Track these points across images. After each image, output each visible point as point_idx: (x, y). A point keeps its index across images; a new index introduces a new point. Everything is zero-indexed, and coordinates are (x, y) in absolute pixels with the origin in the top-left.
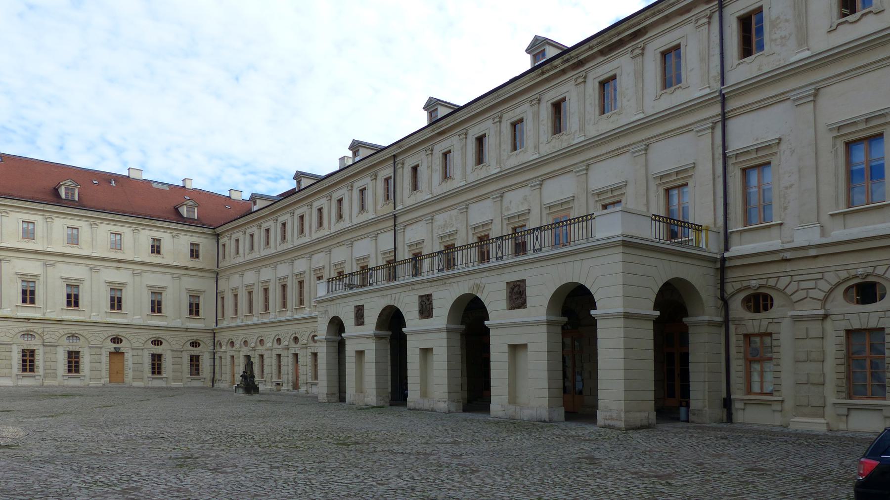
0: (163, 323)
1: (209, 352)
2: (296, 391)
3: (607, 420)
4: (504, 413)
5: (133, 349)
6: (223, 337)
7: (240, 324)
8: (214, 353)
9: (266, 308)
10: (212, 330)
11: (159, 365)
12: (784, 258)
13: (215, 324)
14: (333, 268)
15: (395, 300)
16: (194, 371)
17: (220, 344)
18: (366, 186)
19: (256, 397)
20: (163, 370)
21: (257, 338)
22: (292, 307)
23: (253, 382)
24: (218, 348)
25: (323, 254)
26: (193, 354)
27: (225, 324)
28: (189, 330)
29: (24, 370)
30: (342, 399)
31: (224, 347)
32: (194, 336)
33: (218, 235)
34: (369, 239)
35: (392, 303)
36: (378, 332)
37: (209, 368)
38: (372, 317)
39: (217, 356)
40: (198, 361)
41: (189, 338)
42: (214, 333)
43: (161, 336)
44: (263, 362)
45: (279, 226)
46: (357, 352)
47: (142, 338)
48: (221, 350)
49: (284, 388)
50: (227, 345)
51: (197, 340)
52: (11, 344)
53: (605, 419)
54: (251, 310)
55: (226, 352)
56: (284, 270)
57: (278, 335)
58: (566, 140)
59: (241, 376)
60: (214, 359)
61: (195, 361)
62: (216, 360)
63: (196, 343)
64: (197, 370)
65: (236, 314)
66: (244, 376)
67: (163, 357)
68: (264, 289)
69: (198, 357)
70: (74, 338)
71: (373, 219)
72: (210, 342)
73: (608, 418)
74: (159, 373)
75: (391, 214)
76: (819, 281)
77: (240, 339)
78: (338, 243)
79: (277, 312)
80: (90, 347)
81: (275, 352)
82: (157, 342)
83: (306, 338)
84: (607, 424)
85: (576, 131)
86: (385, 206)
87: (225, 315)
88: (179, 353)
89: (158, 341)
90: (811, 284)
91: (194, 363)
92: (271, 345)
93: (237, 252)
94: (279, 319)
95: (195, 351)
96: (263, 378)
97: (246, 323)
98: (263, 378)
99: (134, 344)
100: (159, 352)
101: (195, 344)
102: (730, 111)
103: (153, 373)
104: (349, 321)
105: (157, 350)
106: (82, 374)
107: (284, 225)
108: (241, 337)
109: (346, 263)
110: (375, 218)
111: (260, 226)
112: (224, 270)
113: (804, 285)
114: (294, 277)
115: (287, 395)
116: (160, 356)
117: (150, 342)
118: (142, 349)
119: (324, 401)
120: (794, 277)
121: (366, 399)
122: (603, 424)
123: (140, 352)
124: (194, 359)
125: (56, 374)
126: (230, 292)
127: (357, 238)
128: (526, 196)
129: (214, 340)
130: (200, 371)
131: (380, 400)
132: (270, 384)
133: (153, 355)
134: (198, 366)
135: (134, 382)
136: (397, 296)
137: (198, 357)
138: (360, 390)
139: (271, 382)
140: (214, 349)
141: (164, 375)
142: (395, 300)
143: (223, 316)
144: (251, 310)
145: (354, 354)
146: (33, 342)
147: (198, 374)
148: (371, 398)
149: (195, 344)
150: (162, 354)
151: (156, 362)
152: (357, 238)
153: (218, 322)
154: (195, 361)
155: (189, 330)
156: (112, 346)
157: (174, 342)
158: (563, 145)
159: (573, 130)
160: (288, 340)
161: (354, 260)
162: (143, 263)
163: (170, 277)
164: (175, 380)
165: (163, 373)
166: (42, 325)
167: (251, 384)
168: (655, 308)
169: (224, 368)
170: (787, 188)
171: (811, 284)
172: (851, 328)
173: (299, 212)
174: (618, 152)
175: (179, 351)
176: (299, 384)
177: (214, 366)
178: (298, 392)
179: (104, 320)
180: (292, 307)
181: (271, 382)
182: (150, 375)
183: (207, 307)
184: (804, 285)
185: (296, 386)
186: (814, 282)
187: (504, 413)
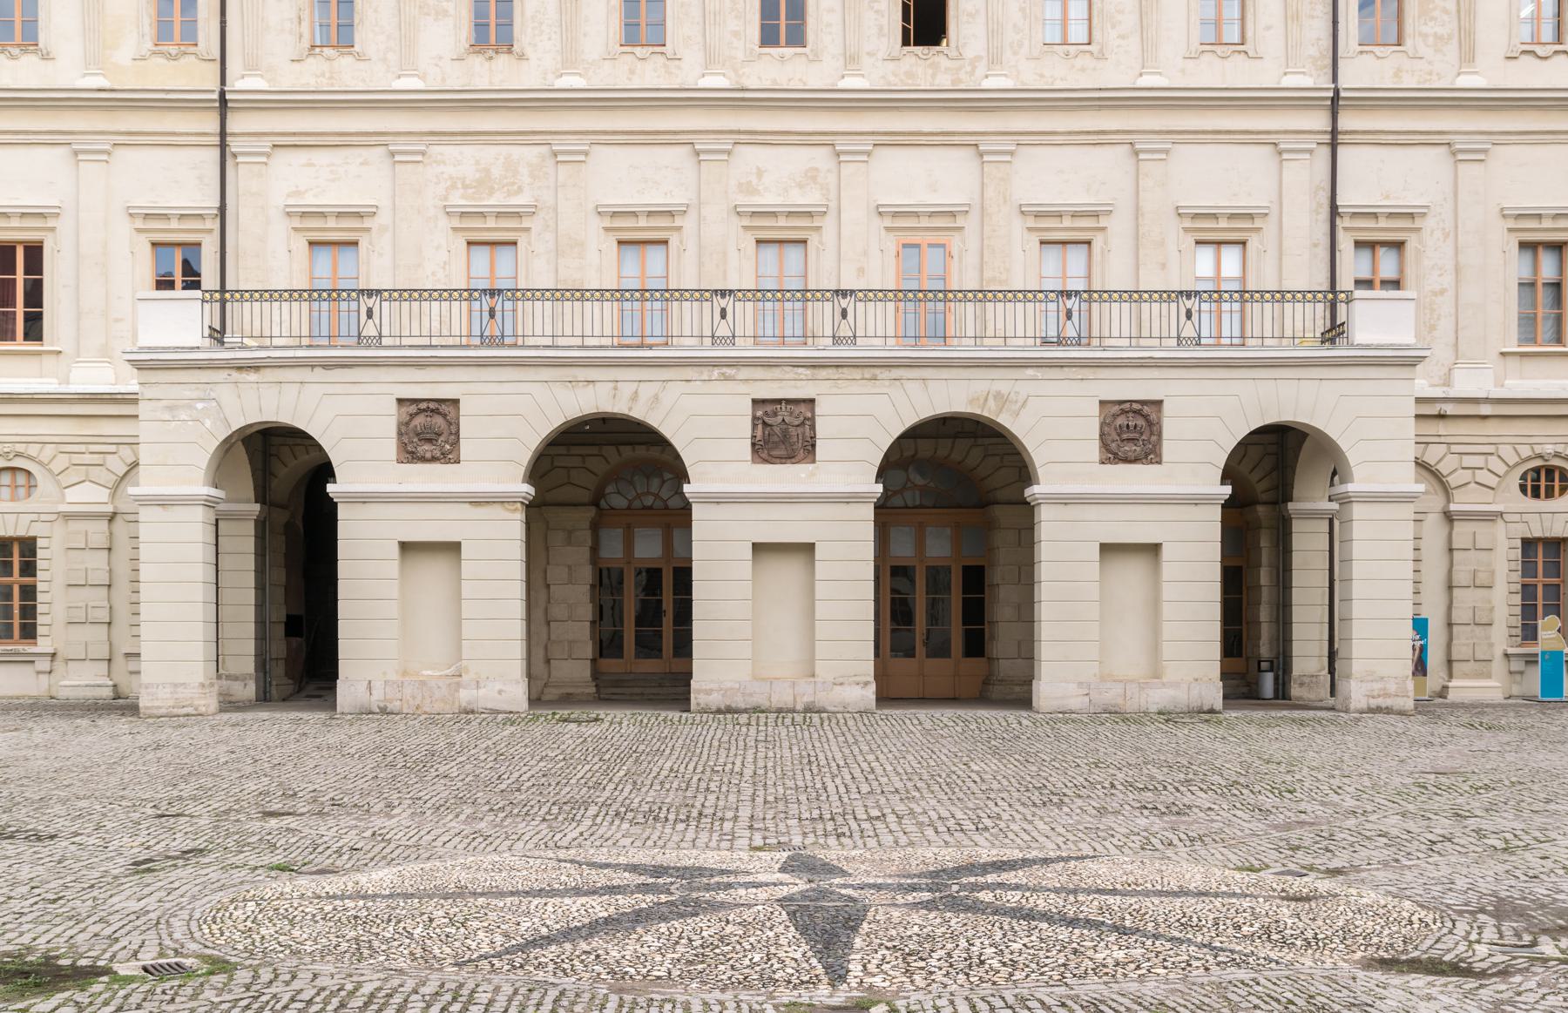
3: (1373, 697)
4: (1086, 699)
12: (1442, 413)
53: (1368, 696)
58: (947, 69)
73: (1375, 693)
76: (1490, 457)
84: (1372, 706)
85: (978, 58)
90: (1477, 461)
102: (1346, 132)
113: (1469, 461)
120: (1452, 446)
122: (1365, 706)
128: (817, 169)
158: (937, 82)
159: (969, 53)
168: (1223, 481)
170: (1435, 294)
171: (1477, 461)
172: (1530, 536)
174: (1098, 138)
184: (1469, 461)
186: (1483, 457)
187: (1086, 699)
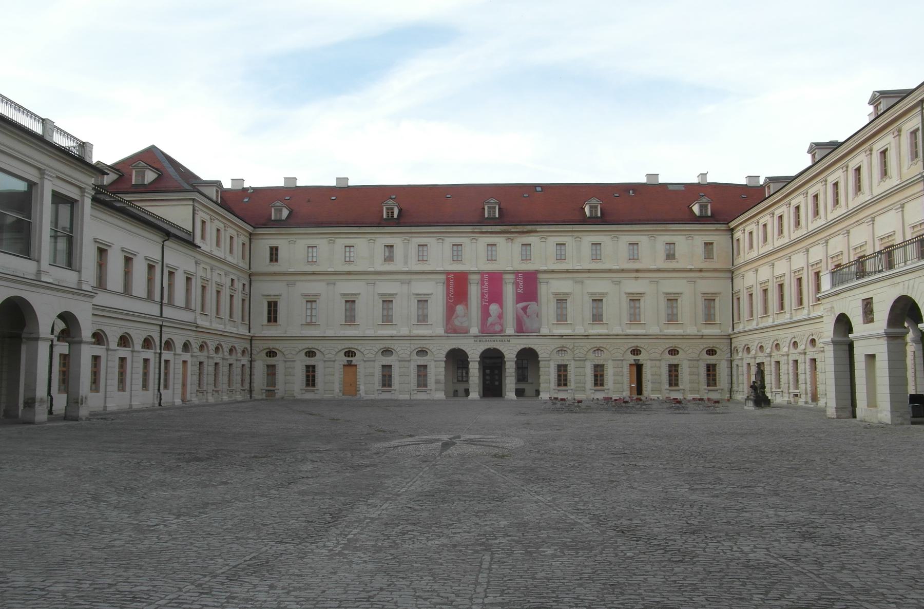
0: (679, 331)
1: (727, 360)
2: (815, 403)
5: (651, 360)
6: (739, 342)
7: (755, 327)
8: (731, 361)
9: (782, 307)
10: (729, 335)
11: (677, 376)
13: (731, 329)
14: (852, 252)
15: (908, 288)
16: (711, 382)
17: (737, 350)
18: (888, 146)
19: (766, 411)
20: (680, 382)
21: (773, 343)
22: (809, 304)
23: (763, 393)
24: (735, 357)
25: (841, 236)
26: (709, 362)
27: (739, 328)
28: (704, 337)
29: (559, 385)
30: (854, 416)
31: (740, 354)
32: (710, 344)
33: (732, 230)
34: (893, 211)
35: (905, 294)
36: (892, 330)
37: (727, 377)
38: (882, 313)
39: (734, 364)
40: (715, 370)
41: (705, 346)
42: (731, 339)
43: (677, 345)
44: (797, 369)
45: (792, 210)
46: (867, 356)
47: (659, 347)
48: (738, 357)
49: (801, 401)
50: (743, 352)
51: (714, 347)
52: (549, 361)
54: (766, 310)
55: (742, 359)
56: (799, 261)
57: (794, 337)
59: (751, 387)
60: (731, 367)
61: (711, 370)
62: (733, 369)
63: (712, 350)
64: (715, 380)
65: (752, 316)
66: (753, 387)
67: (680, 367)
68: (779, 285)
69: (714, 365)
70: (599, 352)
71: (897, 186)
72: (726, 349)
74: (677, 385)
75: (920, 176)
77: (756, 344)
78: (857, 221)
79: (793, 311)
80: (613, 360)
81: (791, 358)
82: (673, 352)
83: (770, 345)
86: (912, 167)
87: (742, 318)
88: (696, 362)
89: (675, 350)
91: (711, 373)
92: (787, 350)
93: (751, 246)
94: (795, 319)
95: (711, 360)
96: (779, 388)
97: (761, 326)
98: (779, 388)
99: (652, 355)
100: (675, 362)
101: (711, 352)
103: (670, 385)
104: (856, 319)
105: (674, 360)
106: (606, 387)
107: (798, 208)
108: (757, 342)
109: (867, 245)
110: (899, 185)
111: (773, 214)
112: (739, 268)
114: (793, 274)
115: (805, 408)
116: (676, 366)
117: (667, 352)
118: (660, 360)
119: (833, 417)
121: (880, 415)
123: (657, 363)
124: (711, 368)
125: (585, 387)
126: (745, 291)
127: (879, 213)
129: (731, 346)
130: (717, 382)
131: (898, 417)
132: (787, 395)
133: (670, 366)
134: (715, 375)
135: (652, 394)
136: (907, 283)
137: (714, 365)
138: (872, 402)
139: (789, 393)
140: (731, 357)
141: (681, 387)
142: (908, 288)
143: (739, 319)
144: (766, 310)
145: (863, 358)
146: (566, 358)
147: (715, 385)
148: (884, 413)
149: (711, 352)
150: (678, 365)
151: (673, 373)
152: (879, 213)
153: (735, 325)
154: (711, 370)
155: (704, 337)
156: (631, 358)
157: (691, 351)
160: (804, 343)
161: (876, 239)
162: (659, 270)
163: (684, 281)
164: (692, 391)
165: (680, 384)
166: (573, 341)
167: (760, 395)
169: (741, 377)
173: (812, 192)
175: (695, 360)
176: (819, 396)
177: (731, 375)
178: (817, 404)
179: (624, 333)
180: (809, 304)
181: (789, 393)
182: (667, 387)
183: (722, 310)
185: (815, 398)
